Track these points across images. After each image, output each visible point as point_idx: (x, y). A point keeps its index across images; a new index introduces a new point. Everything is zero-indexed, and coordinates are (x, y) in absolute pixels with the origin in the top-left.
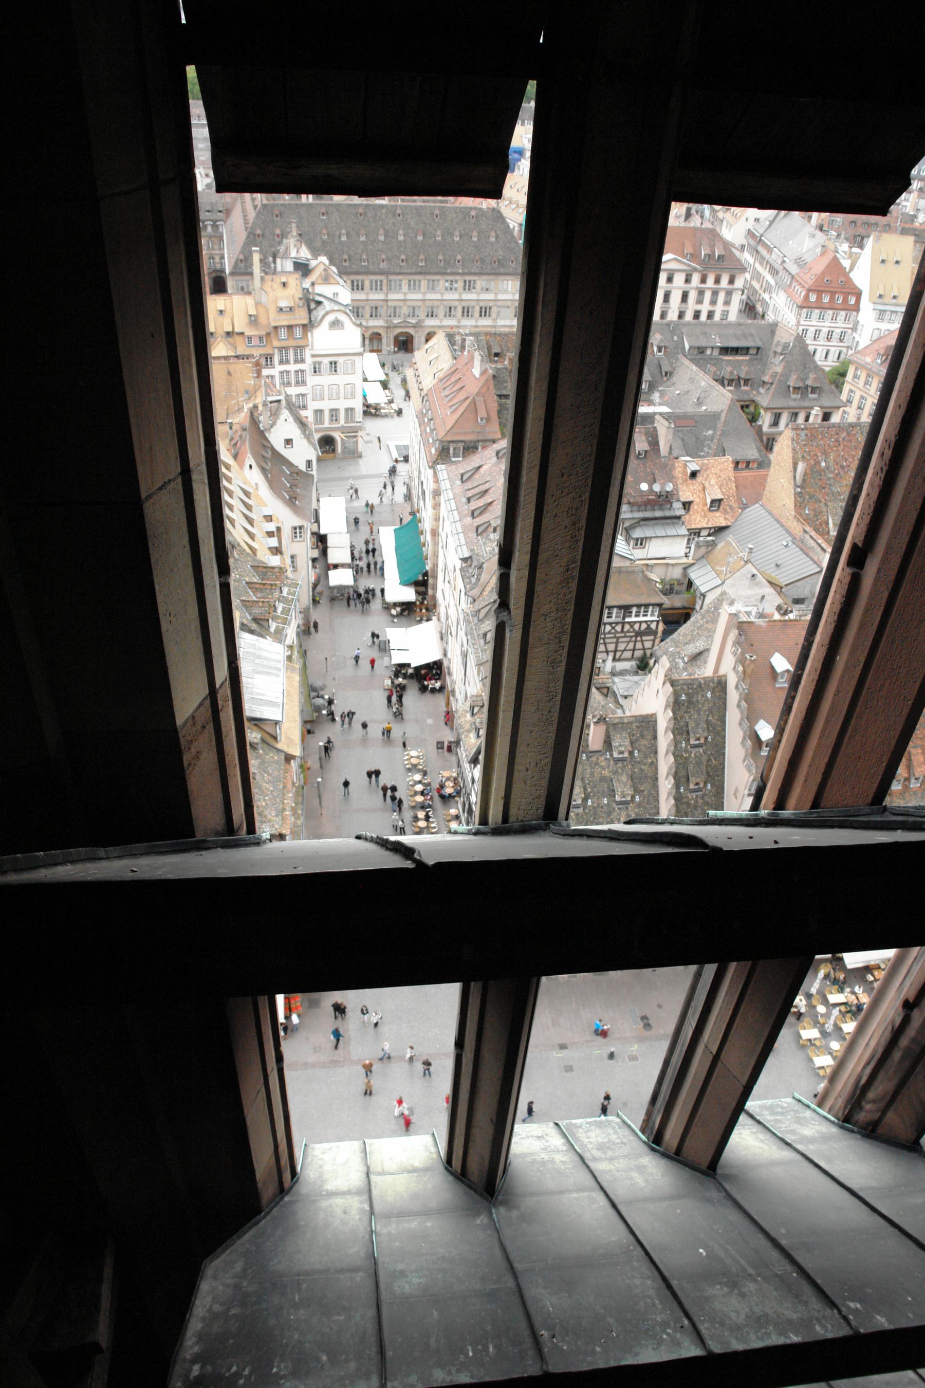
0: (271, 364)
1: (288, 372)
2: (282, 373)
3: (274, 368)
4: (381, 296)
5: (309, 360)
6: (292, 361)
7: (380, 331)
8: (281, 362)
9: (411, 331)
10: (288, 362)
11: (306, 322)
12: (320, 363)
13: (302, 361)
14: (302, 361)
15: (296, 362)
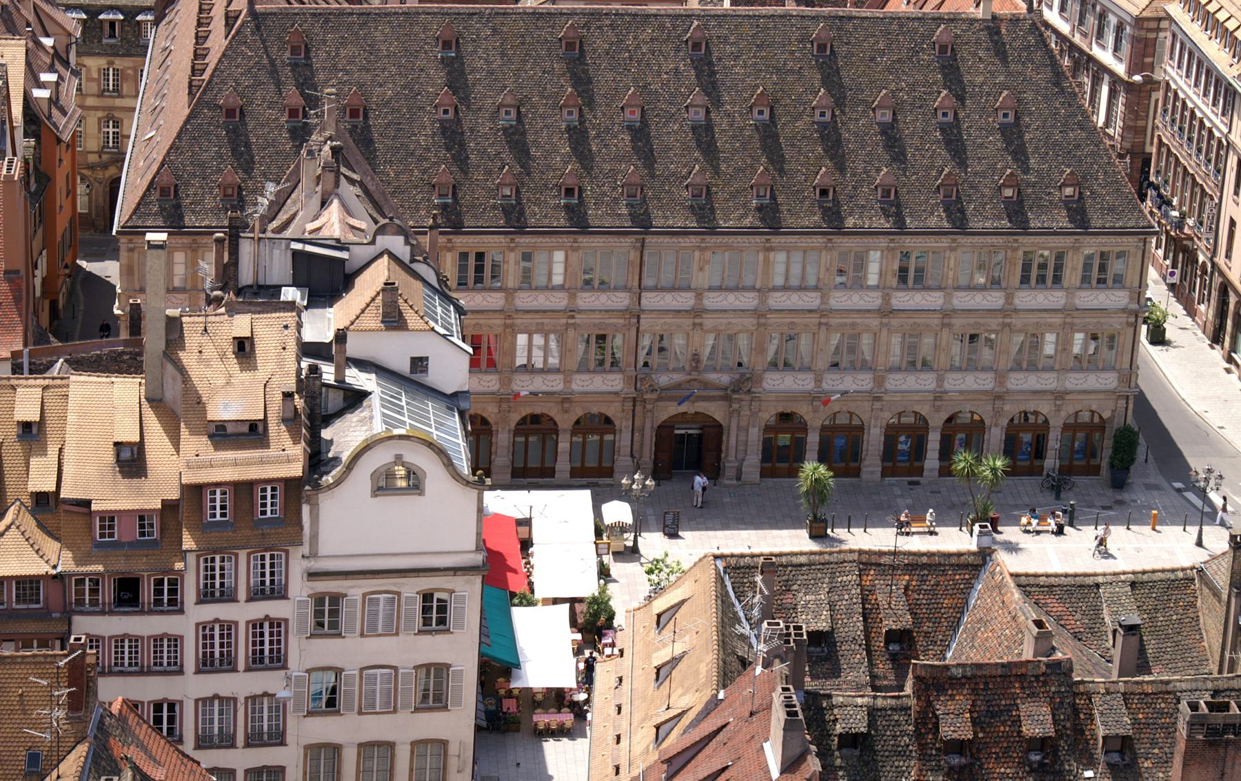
0: (172, 602)
1: (228, 628)
2: (205, 630)
3: (181, 611)
4: (621, 300)
5: (299, 589)
6: (242, 594)
7: (612, 411)
8: (207, 596)
9: (716, 411)
10: (228, 596)
11: (296, 470)
12: (336, 599)
13: (278, 592)
14: (278, 592)
15: (257, 594)
